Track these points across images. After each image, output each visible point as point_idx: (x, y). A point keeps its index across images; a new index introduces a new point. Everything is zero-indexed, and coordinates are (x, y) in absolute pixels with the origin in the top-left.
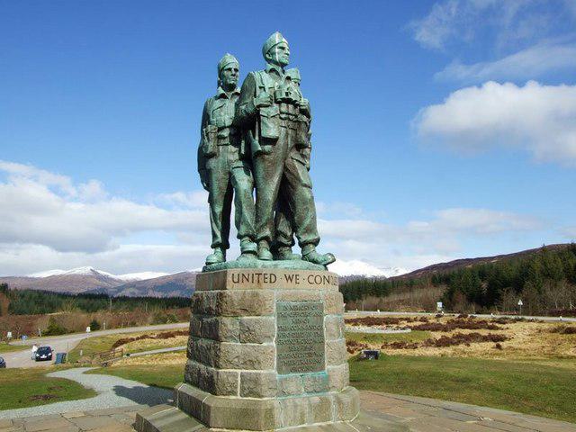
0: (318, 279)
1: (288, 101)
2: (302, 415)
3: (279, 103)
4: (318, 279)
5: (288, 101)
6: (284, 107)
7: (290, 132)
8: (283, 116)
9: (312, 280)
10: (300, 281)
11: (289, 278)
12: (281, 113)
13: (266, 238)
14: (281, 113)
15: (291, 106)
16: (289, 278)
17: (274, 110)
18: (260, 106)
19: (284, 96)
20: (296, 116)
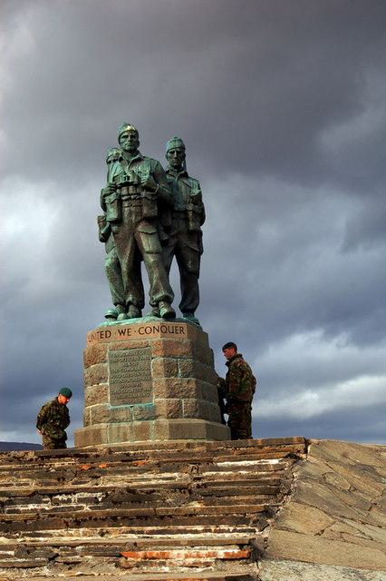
0: (148, 330)
1: (127, 184)
2: (125, 434)
3: (120, 188)
4: (148, 330)
5: (127, 184)
6: (124, 191)
7: (133, 209)
8: (124, 198)
9: (142, 331)
10: (132, 333)
11: (122, 333)
12: (121, 196)
13: (130, 303)
14: (124, 196)
15: (131, 188)
16: (122, 333)
17: (112, 197)
18: (105, 196)
19: (122, 181)
20: (139, 194)
